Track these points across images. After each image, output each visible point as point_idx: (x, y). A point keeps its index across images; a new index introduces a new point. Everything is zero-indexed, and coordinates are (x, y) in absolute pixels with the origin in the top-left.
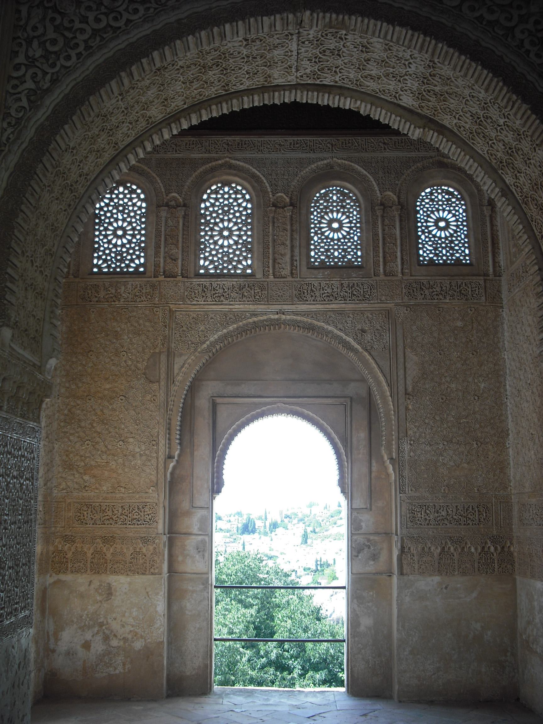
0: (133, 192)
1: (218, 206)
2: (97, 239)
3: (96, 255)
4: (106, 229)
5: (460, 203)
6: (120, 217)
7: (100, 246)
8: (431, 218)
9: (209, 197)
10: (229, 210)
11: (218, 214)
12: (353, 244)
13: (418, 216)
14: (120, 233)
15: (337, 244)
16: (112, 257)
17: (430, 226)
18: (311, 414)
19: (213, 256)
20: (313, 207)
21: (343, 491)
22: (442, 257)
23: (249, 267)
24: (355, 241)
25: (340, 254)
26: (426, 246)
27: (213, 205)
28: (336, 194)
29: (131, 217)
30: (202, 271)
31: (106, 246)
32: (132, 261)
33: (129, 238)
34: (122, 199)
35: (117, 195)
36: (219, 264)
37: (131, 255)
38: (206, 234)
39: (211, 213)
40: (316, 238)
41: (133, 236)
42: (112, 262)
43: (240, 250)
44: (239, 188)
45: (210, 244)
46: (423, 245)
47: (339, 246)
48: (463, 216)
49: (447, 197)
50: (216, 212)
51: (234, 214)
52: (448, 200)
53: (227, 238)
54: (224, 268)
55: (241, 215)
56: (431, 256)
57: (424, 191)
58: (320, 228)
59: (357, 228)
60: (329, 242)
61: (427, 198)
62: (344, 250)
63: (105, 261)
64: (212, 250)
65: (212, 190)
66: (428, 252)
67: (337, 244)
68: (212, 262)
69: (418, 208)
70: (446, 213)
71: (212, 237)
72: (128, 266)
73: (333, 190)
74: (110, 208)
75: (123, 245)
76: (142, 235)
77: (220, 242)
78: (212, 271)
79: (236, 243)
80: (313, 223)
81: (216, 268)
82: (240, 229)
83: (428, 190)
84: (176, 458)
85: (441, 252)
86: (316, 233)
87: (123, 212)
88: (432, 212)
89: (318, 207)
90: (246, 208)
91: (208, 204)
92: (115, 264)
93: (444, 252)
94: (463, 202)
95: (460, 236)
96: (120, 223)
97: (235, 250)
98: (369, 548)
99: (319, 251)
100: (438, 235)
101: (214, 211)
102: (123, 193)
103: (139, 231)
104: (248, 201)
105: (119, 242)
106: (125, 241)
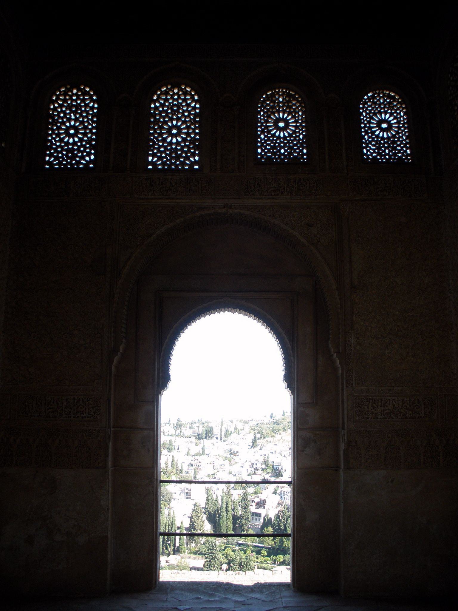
0: (85, 93)
1: (168, 106)
2: (50, 138)
3: (48, 152)
4: (59, 128)
5: (401, 107)
6: (73, 117)
7: (52, 144)
8: (374, 120)
9: (159, 98)
10: (178, 109)
11: (167, 114)
12: (298, 142)
13: (362, 117)
14: (72, 132)
15: (283, 142)
16: (63, 154)
17: (373, 127)
18: (258, 309)
19: (162, 152)
20: (260, 107)
21: (290, 386)
22: (385, 156)
23: (196, 163)
24: (300, 139)
25: (285, 151)
26: (370, 145)
27: (162, 105)
28: (282, 95)
29: (83, 117)
30: (150, 167)
31: (58, 144)
32: (83, 157)
33: (81, 136)
34: (76, 101)
35: (71, 97)
36: (167, 160)
37: (82, 152)
38: (155, 132)
39: (161, 112)
40: (262, 136)
41: (85, 134)
42: (64, 160)
43: (188, 147)
44: (188, 89)
45: (159, 141)
46: (368, 144)
47: (285, 144)
48: (404, 119)
49: (388, 100)
50: (166, 112)
51: (183, 114)
52: (388, 103)
53: (176, 136)
54: (172, 164)
55: (190, 114)
56: (374, 155)
57: (367, 95)
58: (267, 127)
59: (303, 127)
60: (276, 140)
61: (370, 101)
62: (289, 148)
63: (57, 158)
64: (160, 147)
65: (162, 91)
66: (371, 151)
67: (283, 142)
68: (160, 158)
69: (361, 111)
70: (388, 116)
71: (161, 134)
72: (79, 163)
73: (279, 92)
74: (64, 109)
75: (75, 143)
76: (93, 134)
77: (169, 140)
78: (159, 167)
79: (184, 140)
80: (260, 122)
81: (163, 164)
82: (188, 128)
83: (370, 95)
84: (121, 351)
85: (384, 151)
86: (262, 132)
87: (75, 113)
88: (375, 114)
89: (265, 107)
90: (194, 108)
91: (158, 104)
92: (66, 161)
93: (387, 151)
94: (404, 106)
95: (402, 137)
96: (73, 123)
97: (183, 147)
98: (315, 442)
99: (266, 148)
100: (381, 135)
101: (163, 111)
102: (76, 95)
103: (91, 130)
104: (196, 102)
105: (71, 141)
106: (76, 139)
